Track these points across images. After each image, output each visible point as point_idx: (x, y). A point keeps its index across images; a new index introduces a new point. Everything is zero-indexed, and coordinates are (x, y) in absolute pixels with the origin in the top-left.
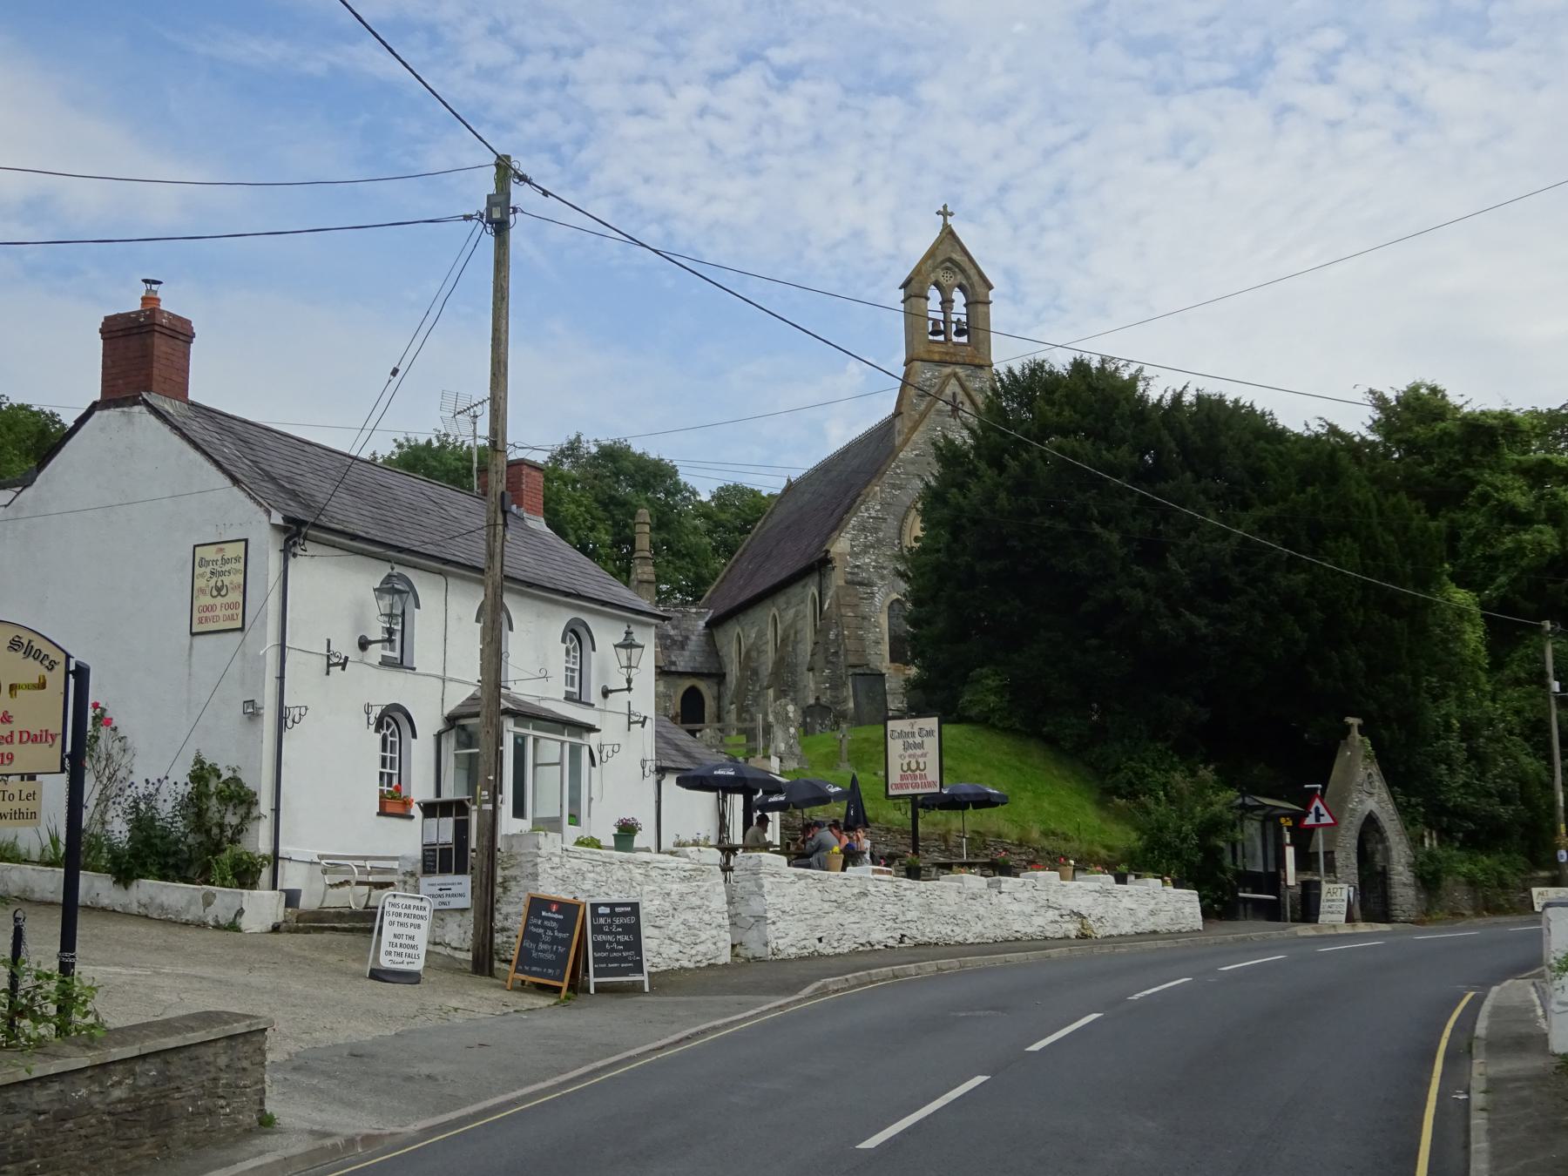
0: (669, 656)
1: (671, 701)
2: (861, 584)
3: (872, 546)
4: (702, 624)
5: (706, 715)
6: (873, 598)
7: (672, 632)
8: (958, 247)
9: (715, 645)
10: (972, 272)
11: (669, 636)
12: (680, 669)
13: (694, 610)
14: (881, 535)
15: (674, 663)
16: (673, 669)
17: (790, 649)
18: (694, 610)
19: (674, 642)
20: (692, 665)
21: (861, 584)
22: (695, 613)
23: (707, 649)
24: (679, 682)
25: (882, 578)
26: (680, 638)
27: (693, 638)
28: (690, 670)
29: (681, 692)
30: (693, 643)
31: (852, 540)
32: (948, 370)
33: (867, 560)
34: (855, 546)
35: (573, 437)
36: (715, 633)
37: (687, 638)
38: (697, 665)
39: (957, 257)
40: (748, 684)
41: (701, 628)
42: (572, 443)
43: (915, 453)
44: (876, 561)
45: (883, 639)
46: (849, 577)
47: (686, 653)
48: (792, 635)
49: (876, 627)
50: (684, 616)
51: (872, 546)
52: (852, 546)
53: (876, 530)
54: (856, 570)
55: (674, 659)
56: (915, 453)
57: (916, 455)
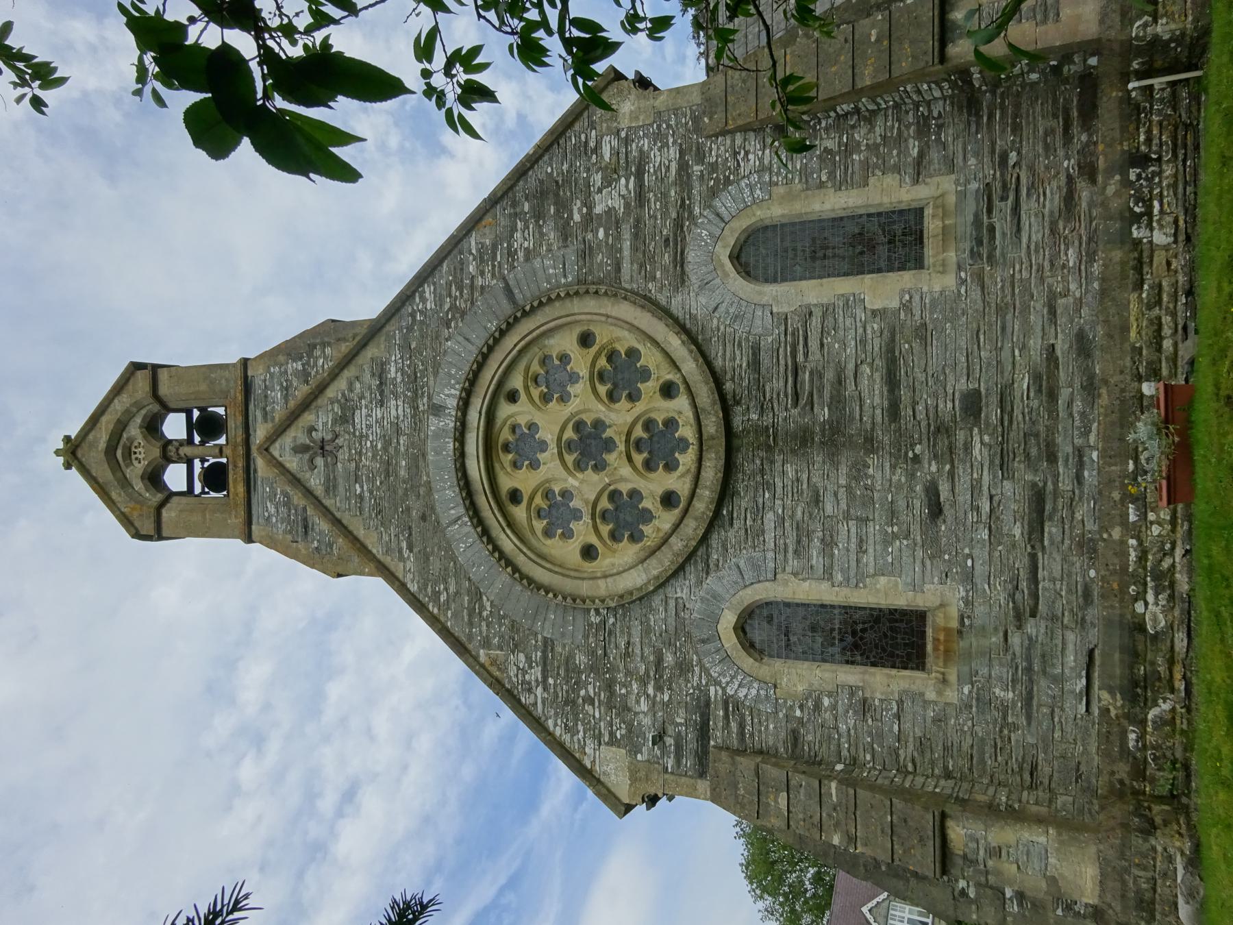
2: (703, 732)
3: (609, 686)
6: (738, 705)
8: (91, 437)
10: (119, 406)
14: (581, 659)
21: (703, 732)
25: (684, 668)
31: (598, 738)
32: (260, 463)
33: (644, 706)
34: (612, 734)
39: (102, 436)
43: (406, 553)
44: (644, 682)
45: (852, 690)
46: (688, 762)
49: (818, 706)
51: (609, 686)
52: (613, 741)
53: (571, 669)
54: (669, 741)
56: (406, 553)
57: (410, 549)
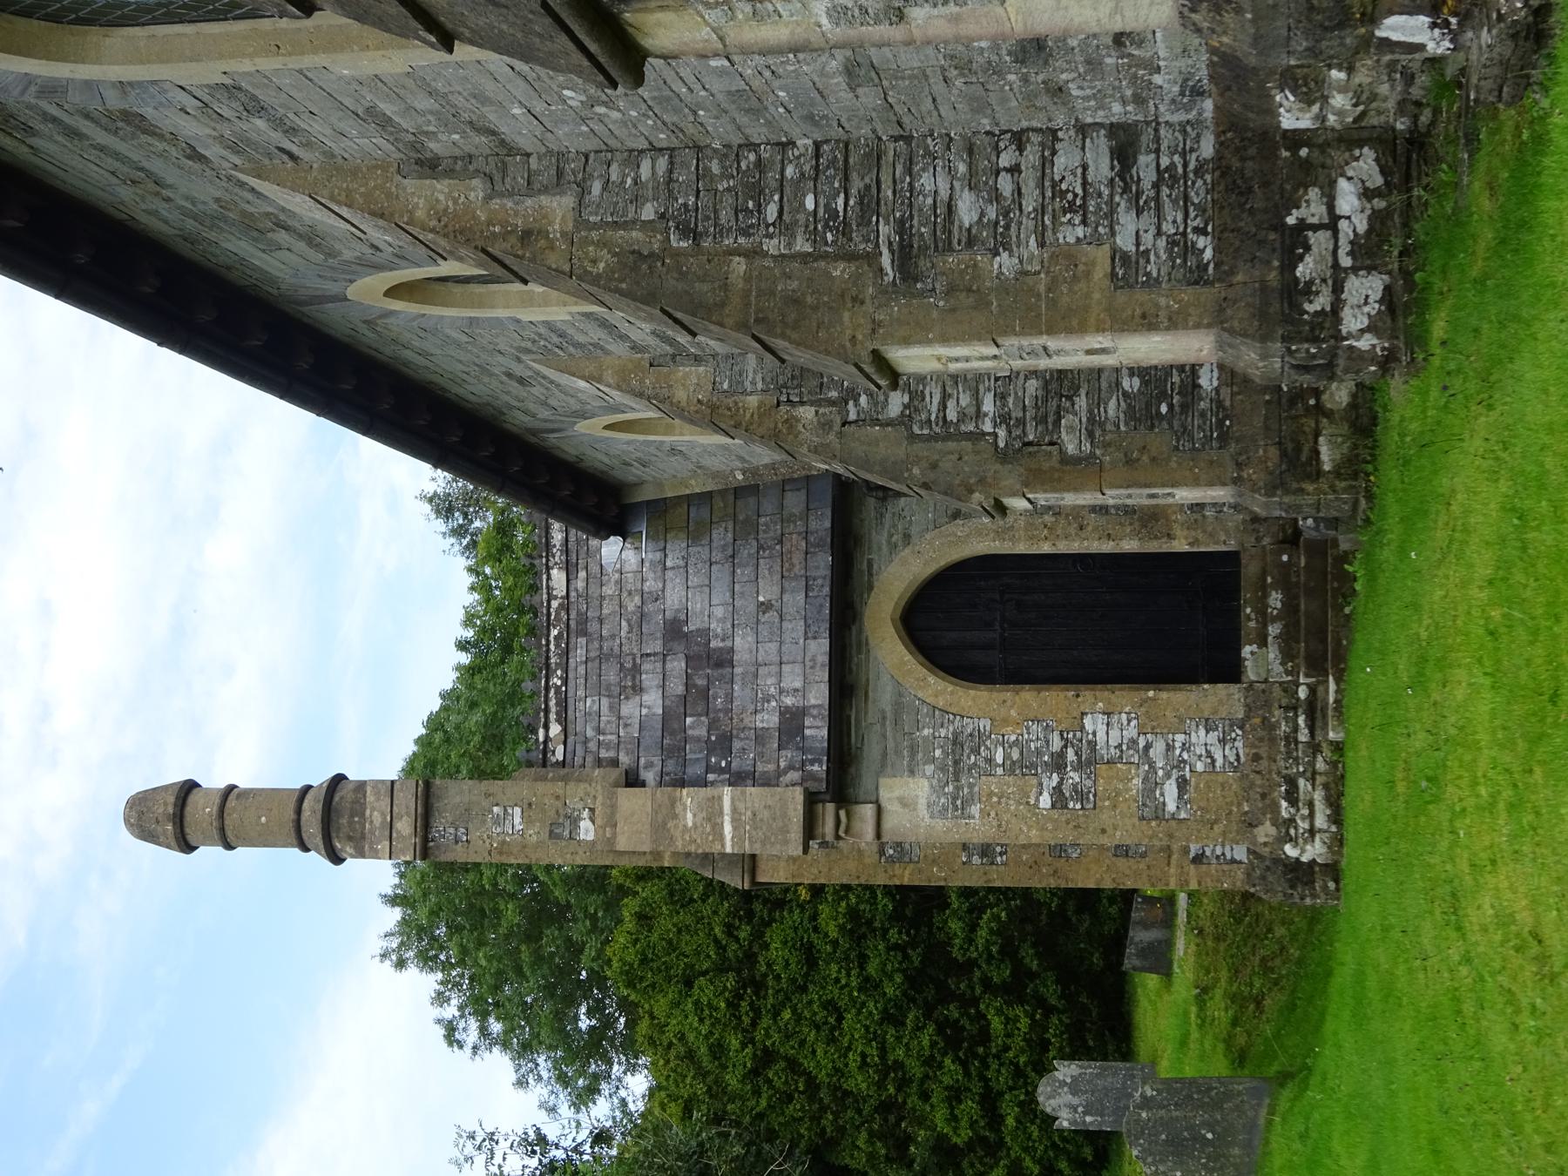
0: (760, 737)
1: (979, 738)
4: (611, 548)
5: (1046, 548)
7: (653, 700)
9: (709, 495)
11: (670, 720)
12: (819, 696)
13: (558, 576)
15: (792, 722)
16: (817, 730)
17: (558, 208)
18: (558, 576)
19: (694, 697)
20: (795, 628)
22: (570, 569)
23: (721, 535)
24: (882, 696)
26: (677, 665)
27: (674, 598)
28: (820, 648)
29: (934, 688)
30: (697, 604)
35: (427, 508)
36: (647, 494)
37: (674, 630)
38: (795, 600)
40: (870, 420)
41: (631, 557)
42: (438, 512)
47: (742, 643)
48: (441, 189)
50: (583, 620)
55: (769, 719)
